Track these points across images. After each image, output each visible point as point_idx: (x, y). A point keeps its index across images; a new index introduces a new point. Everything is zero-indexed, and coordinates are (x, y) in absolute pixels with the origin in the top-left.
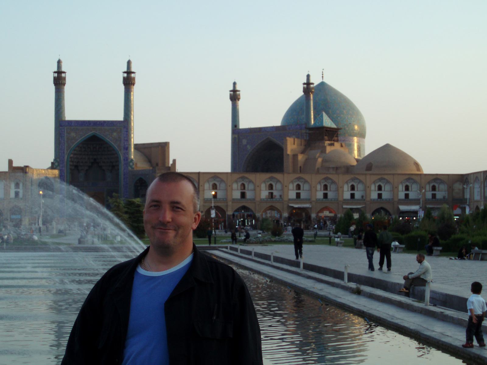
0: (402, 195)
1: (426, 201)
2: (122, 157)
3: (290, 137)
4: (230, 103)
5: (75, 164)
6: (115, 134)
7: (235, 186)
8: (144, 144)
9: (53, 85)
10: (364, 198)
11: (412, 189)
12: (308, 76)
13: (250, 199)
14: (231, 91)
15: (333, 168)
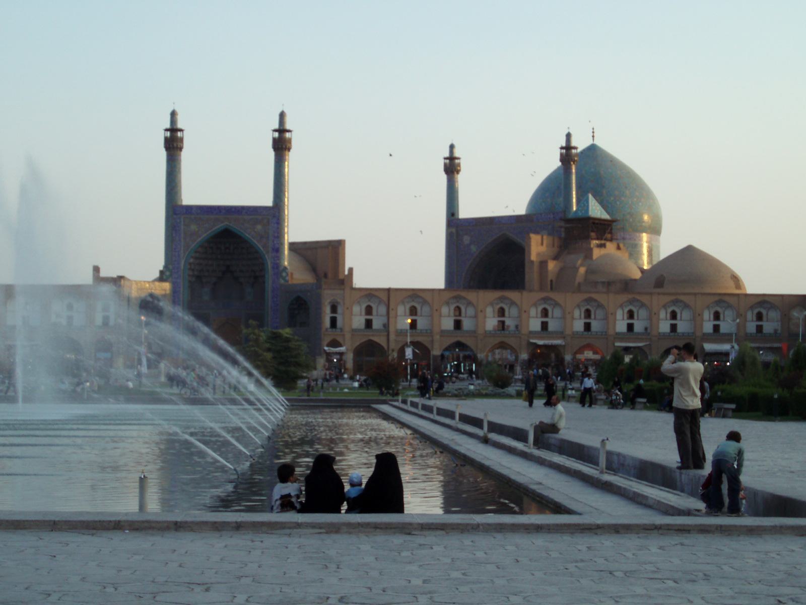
0: (708, 327)
1: (749, 337)
2: (269, 263)
3: (536, 233)
4: (444, 177)
5: (196, 273)
6: (259, 227)
7: (445, 310)
8: (305, 243)
9: (164, 149)
10: (649, 331)
11: (724, 319)
12: (569, 136)
13: (467, 332)
14: (445, 159)
15: (603, 283)
